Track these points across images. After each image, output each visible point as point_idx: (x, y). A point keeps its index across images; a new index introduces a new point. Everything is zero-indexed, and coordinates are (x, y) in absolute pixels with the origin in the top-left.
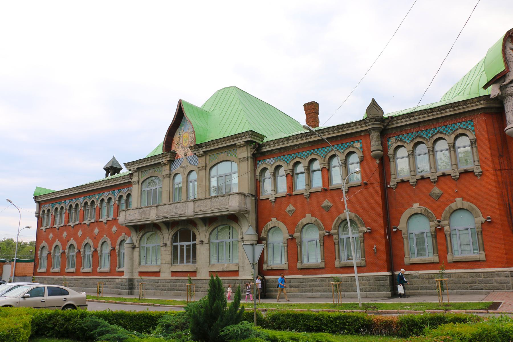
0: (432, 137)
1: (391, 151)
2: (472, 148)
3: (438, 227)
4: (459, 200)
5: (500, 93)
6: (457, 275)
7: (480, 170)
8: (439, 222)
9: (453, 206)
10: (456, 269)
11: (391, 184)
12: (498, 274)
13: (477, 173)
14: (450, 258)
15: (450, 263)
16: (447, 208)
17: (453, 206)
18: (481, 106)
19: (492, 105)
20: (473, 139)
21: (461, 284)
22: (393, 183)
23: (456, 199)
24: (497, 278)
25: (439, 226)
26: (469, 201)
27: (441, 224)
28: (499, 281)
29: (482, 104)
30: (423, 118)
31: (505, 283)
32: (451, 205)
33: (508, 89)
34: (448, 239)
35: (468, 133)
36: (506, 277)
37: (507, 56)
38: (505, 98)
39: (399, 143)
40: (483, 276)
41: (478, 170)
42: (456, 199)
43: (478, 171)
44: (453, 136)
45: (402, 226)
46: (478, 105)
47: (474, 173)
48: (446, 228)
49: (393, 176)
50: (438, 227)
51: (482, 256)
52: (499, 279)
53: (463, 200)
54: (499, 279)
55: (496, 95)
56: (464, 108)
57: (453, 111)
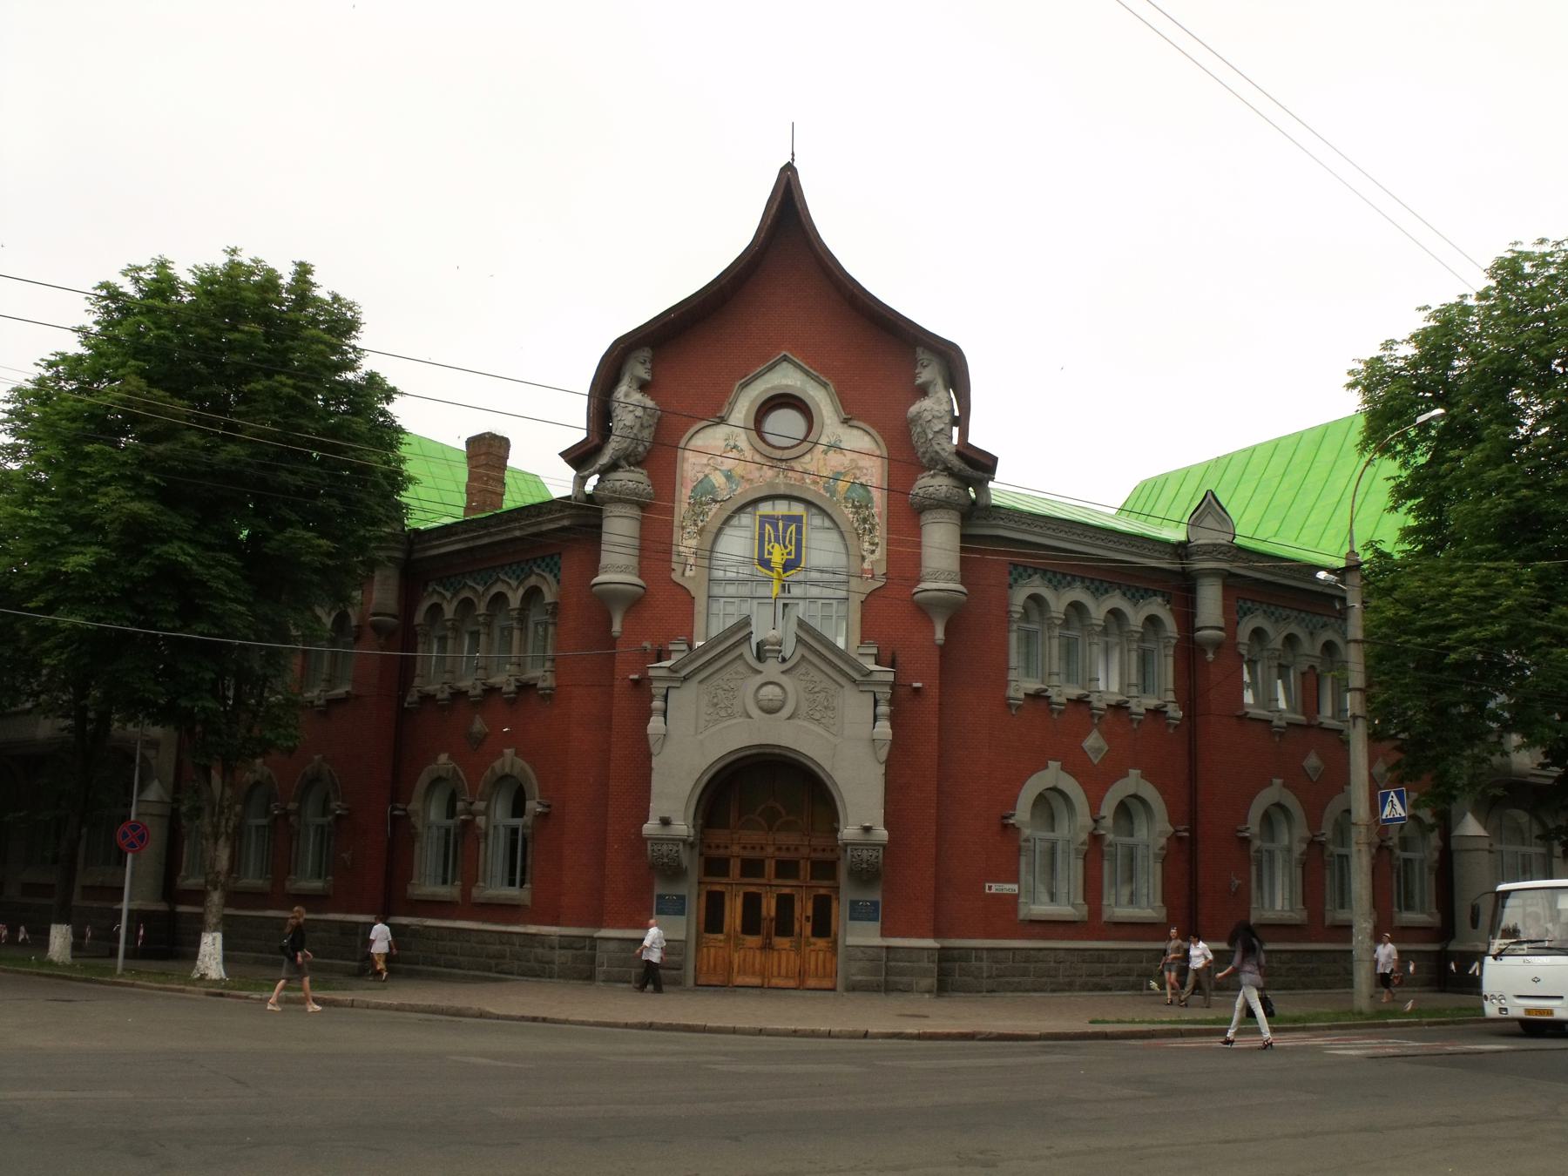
0: (488, 589)
1: (419, 618)
4: (509, 752)
11: (409, 699)
16: (488, 772)
17: (497, 764)
18: (566, 523)
22: (412, 698)
25: (470, 813)
27: (474, 807)
30: (473, 538)
34: (482, 846)
35: (545, 589)
39: (435, 599)
44: (521, 591)
45: (415, 805)
46: (562, 518)
49: (417, 681)
52: (540, 951)
56: (540, 523)
57: (521, 528)
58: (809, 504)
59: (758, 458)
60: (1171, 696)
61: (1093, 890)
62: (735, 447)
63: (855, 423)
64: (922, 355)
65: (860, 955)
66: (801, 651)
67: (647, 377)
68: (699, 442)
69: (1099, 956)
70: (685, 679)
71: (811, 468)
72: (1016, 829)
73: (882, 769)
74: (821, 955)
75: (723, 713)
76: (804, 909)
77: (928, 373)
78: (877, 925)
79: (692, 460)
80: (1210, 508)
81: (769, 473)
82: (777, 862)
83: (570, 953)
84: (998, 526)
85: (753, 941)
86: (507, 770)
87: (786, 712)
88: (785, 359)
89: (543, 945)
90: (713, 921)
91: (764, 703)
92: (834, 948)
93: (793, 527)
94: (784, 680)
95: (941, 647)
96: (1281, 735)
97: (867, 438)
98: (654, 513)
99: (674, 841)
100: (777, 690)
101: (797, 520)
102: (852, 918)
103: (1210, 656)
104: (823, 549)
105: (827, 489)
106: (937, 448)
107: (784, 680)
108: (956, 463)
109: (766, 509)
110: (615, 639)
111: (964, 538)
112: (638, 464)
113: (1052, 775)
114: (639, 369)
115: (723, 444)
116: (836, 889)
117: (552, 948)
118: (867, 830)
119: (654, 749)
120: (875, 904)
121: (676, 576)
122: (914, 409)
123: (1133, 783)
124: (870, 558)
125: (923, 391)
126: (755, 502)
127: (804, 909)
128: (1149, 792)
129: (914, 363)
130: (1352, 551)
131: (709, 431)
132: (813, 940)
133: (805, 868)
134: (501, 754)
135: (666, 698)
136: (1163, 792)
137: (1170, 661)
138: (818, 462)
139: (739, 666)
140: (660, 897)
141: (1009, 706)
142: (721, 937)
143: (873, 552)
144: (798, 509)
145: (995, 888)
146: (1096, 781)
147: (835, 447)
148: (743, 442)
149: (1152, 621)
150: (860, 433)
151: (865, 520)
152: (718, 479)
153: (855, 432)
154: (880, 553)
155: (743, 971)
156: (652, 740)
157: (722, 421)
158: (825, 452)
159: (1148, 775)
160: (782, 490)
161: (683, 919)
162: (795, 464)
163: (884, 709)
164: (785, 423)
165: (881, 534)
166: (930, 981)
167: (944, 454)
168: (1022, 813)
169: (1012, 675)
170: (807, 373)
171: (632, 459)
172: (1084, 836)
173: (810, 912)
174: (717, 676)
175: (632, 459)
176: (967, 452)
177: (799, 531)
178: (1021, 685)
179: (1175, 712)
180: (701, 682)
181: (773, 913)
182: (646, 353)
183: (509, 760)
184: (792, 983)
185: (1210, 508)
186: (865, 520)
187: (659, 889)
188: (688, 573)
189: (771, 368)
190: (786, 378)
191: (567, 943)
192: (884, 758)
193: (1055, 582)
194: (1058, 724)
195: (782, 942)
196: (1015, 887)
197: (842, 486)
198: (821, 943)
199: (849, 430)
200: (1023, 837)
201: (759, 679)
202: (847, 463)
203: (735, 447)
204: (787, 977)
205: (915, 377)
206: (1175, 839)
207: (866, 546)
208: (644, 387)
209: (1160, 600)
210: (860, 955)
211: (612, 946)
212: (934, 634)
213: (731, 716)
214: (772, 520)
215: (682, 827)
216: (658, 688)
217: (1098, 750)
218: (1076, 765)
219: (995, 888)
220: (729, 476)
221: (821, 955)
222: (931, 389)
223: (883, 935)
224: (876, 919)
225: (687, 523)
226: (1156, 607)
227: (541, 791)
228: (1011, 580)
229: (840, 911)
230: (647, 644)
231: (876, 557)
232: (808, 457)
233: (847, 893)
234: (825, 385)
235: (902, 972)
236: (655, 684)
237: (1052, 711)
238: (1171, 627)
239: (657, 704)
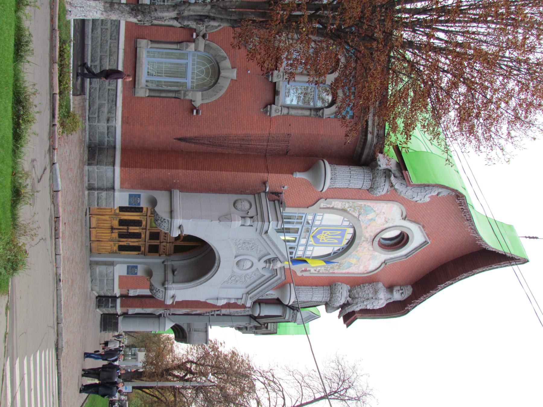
2: (310, 109)
3: (195, 34)
4: (234, 74)
5: (380, 168)
6: (114, 49)
7: (274, 114)
8: (204, 36)
9: (226, 64)
10: (124, 50)
12: (112, 110)
13: (271, 108)
14: (143, 44)
15: (136, 42)
18: (369, 136)
19: (366, 151)
20: (323, 114)
21: (99, 54)
23: (235, 70)
24: (106, 107)
25: (197, 36)
26: (230, 88)
27: (200, 38)
28: (102, 109)
29: (372, 138)
31: (98, 116)
32: (228, 60)
33: (383, 179)
34: (174, 46)
36: (108, 120)
37: (431, 188)
38: (372, 169)
40: (110, 88)
41: (275, 111)
42: (235, 70)
43: (273, 111)
47: (270, 104)
48: (192, 46)
50: (195, 34)
51: (141, 93)
52: (105, 109)
53: (232, 80)
54: (105, 109)
55: (379, 163)
63: (383, 265)
64: (408, 291)
65: (109, 271)
66: (267, 274)
67: (440, 195)
73: (202, 300)
74: (110, 248)
75: (240, 246)
76: (132, 242)
77: (397, 296)
79: (386, 205)
82: (158, 245)
83: (106, 131)
85: (116, 223)
86: (223, 73)
87: (236, 269)
89: (109, 112)
91: (241, 263)
92: (112, 253)
93: (336, 241)
97: (374, 269)
102: (128, 267)
106: (359, 305)
108: (349, 310)
110: (292, 174)
116: (144, 254)
117: (108, 120)
118: (173, 297)
120: (136, 274)
125: (390, 288)
127: (132, 242)
132: (117, 245)
133: (155, 242)
134: (233, 68)
135: (252, 226)
140: (139, 196)
142: (118, 211)
150: (378, 266)
152: (371, 216)
153: (379, 264)
155: (98, 220)
160: (356, 241)
163: (232, 301)
170: (416, 249)
173: (131, 244)
176: (353, 317)
181: (130, 231)
183: (230, 74)
184: (93, 238)
191: (111, 131)
192: (208, 301)
195: (115, 235)
198: (116, 248)
204: (96, 236)
210: (109, 271)
211: (110, 174)
215: (176, 234)
221: (110, 248)
222: (389, 296)
223: (120, 277)
224: (128, 273)
225: (351, 205)
227: (207, 104)
229: (132, 258)
230: (286, 187)
232: (371, 249)
233: (142, 263)
234: (407, 255)
236: (260, 223)
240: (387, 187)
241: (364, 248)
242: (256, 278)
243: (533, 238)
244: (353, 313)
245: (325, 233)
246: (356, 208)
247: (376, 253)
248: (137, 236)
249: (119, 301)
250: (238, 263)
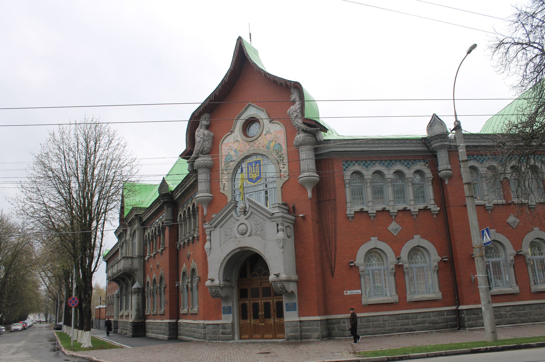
58: (262, 155)
59: (244, 142)
60: (433, 202)
61: (401, 288)
62: (237, 141)
66: (251, 210)
67: (206, 123)
68: (225, 142)
69: (406, 317)
70: (215, 227)
71: (261, 141)
72: (356, 267)
75: (229, 237)
76: (273, 308)
77: (294, 96)
78: (296, 313)
80: (435, 121)
81: (248, 147)
84: (332, 147)
88: (250, 105)
90: (243, 315)
91: (240, 232)
94: (246, 222)
95: (310, 199)
96: (491, 210)
97: (279, 126)
98: (213, 169)
99: (216, 287)
100: (244, 226)
101: (259, 162)
103: (447, 182)
104: (270, 170)
105: (267, 148)
106: (296, 123)
107: (246, 222)
108: (304, 127)
109: (249, 160)
111: (316, 156)
112: (208, 154)
113: (374, 242)
114: (204, 122)
115: (233, 140)
119: (208, 254)
120: (295, 304)
121: (221, 191)
122: (288, 111)
123: (417, 240)
124: (283, 170)
126: (247, 157)
127: (273, 308)
128: (426, 243)
129: (290, 93)
130: (457, 121)
131: (229, 137)
135: (210, 234)
136: (433, 243)
137: (431, 188)
138: (263, 141)
139: (232, 219)
140: (224, 308)
141: (348, 218)
143: (284, 168)
144: (259, 158)
145: (349, 293)
146: (396, 243)
147: (268, 132)
148: (239, 139)
149: (418, 172)
151: (280, 157)
152: (232, 153)
153: (275, 125)
154: (286, 167)
156: (206, 250)
157: (232, 132)
158: (265, 135)
159: (423, 237)
160: (252, 152)
161: (231, 315)
162: (255, 142)
164: (254, 129)
165: (286, 160)
166: (316, 334)
167: (299, 124)
168: (359, 260)
169: (349, 205)
171: (204, 153)
172: (393, 266)
174: (226, 224)
175: (204, 153)
177: (260, 166)
178: (352, 209)
179: (435, 209)
180: (220, 227)
182: (206, 115)
185: (435, 121)
186: (280, 157)
187: (223, 305)
188: (225, 189)
189: (246, 109)
190: (252, 112)
191: (205, 326)
193: (366, 164)
194: (374, 222)
196: (359, 291)
197: (272, 144)
199: (272, 125)
200: (360, 270)
201: (239, 223)
202: (272, 136)
203: (237, 141)
205: (290, 98)
206: (441, 262)
207: (281, 166)
208: (208, 127)
209: (422, 163)
211: (210, 327)
212: (307, 194)
213: (231, 238)
214: (250, 164)
216: (207, 232)
217: (396, 230)
218: (385, 237)
219: (349, 293)
220: (235, 152)
226: (420, 166)
228: (344, 167)
231: (285, 169)
232: (260, 138)
235: (307, 331)
236: (206, 230)
237: (370, 217)
238: (428, 174)
239: (208, 238)
240: (199, 159)
241: (259, 143)
242: (256, 217)
243: (250, 36)
244: (304, 123)
245: (251, 176)
246: (227, 166)
247: (264, 132)
248: (267, 305)
249: (461, 308)
250: (243, 234)
